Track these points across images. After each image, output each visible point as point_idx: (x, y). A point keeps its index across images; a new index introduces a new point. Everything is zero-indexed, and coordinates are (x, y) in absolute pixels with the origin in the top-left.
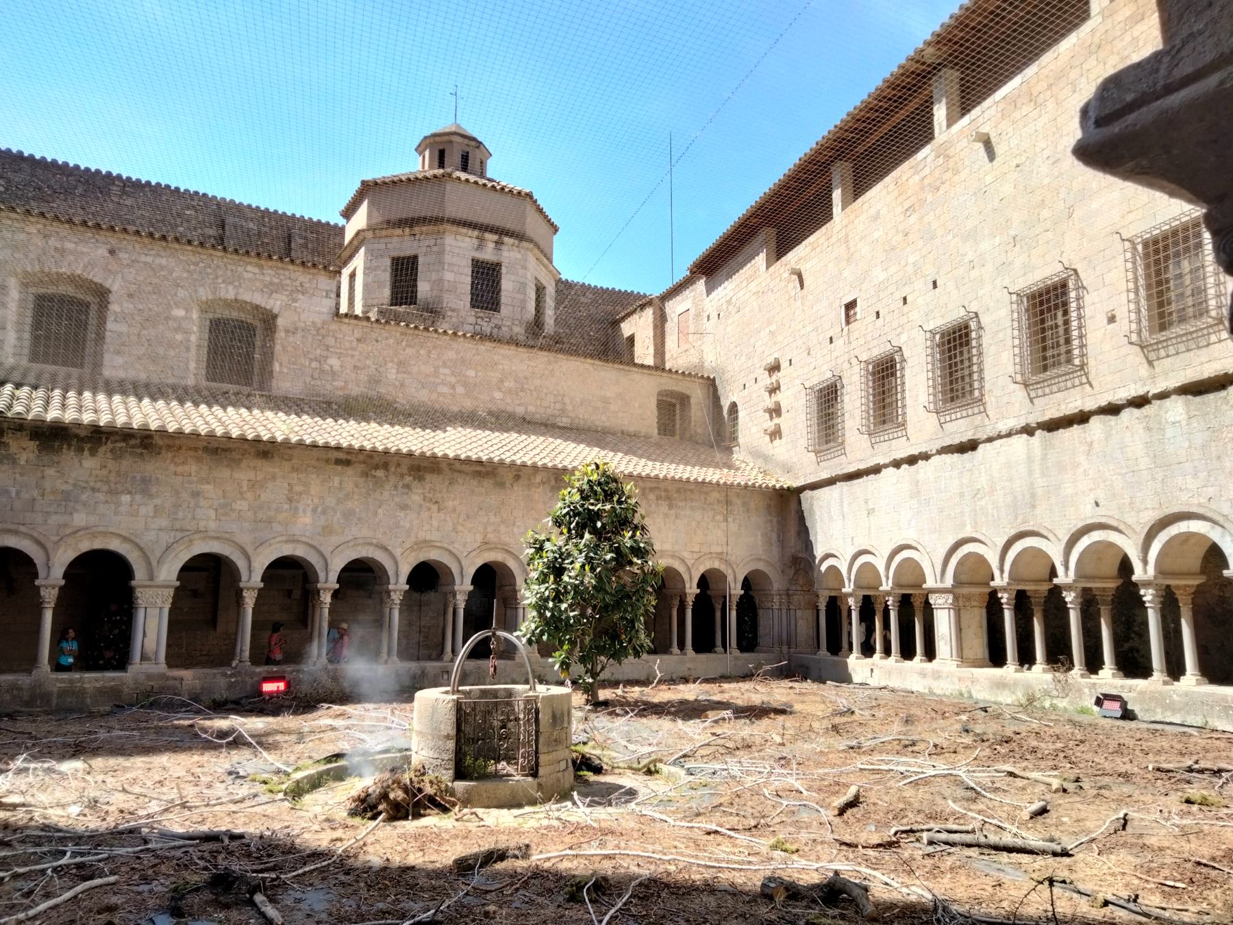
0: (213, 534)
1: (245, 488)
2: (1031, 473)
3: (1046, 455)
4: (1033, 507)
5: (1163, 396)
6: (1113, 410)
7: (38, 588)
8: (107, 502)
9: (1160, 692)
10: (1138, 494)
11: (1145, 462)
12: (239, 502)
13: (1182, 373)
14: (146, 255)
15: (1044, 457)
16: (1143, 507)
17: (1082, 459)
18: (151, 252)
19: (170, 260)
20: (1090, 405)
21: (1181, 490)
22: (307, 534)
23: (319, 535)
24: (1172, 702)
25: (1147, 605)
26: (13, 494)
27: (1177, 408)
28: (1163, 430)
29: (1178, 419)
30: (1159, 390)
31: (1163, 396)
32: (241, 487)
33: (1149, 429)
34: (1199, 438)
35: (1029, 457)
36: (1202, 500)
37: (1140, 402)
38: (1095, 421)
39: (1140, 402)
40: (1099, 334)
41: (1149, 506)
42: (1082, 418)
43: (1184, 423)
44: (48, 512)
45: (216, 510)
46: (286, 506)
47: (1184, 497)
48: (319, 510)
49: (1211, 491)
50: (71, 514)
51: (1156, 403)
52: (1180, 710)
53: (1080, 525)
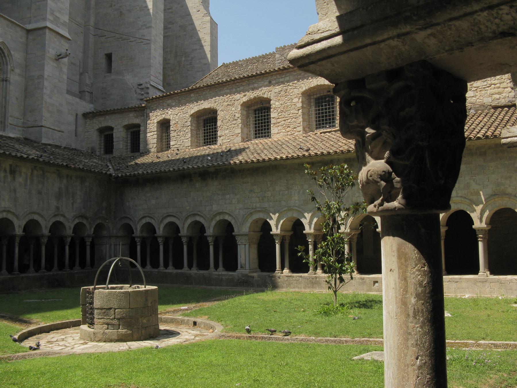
0: (259, 209)
1: (269, 185)
7: (206, 237)
8: (222, 199)
12: (267, 193)
14: (281, 78)
18: (283, 76)
19: (290, 76)
22: (297, 205)
23: (302, 205)
26: (196, 200)
32: (267, 185)
44: (205, 206)
45: (259, 197)
46: (287, 192)
48: (301, 192)
50: (212, 205)
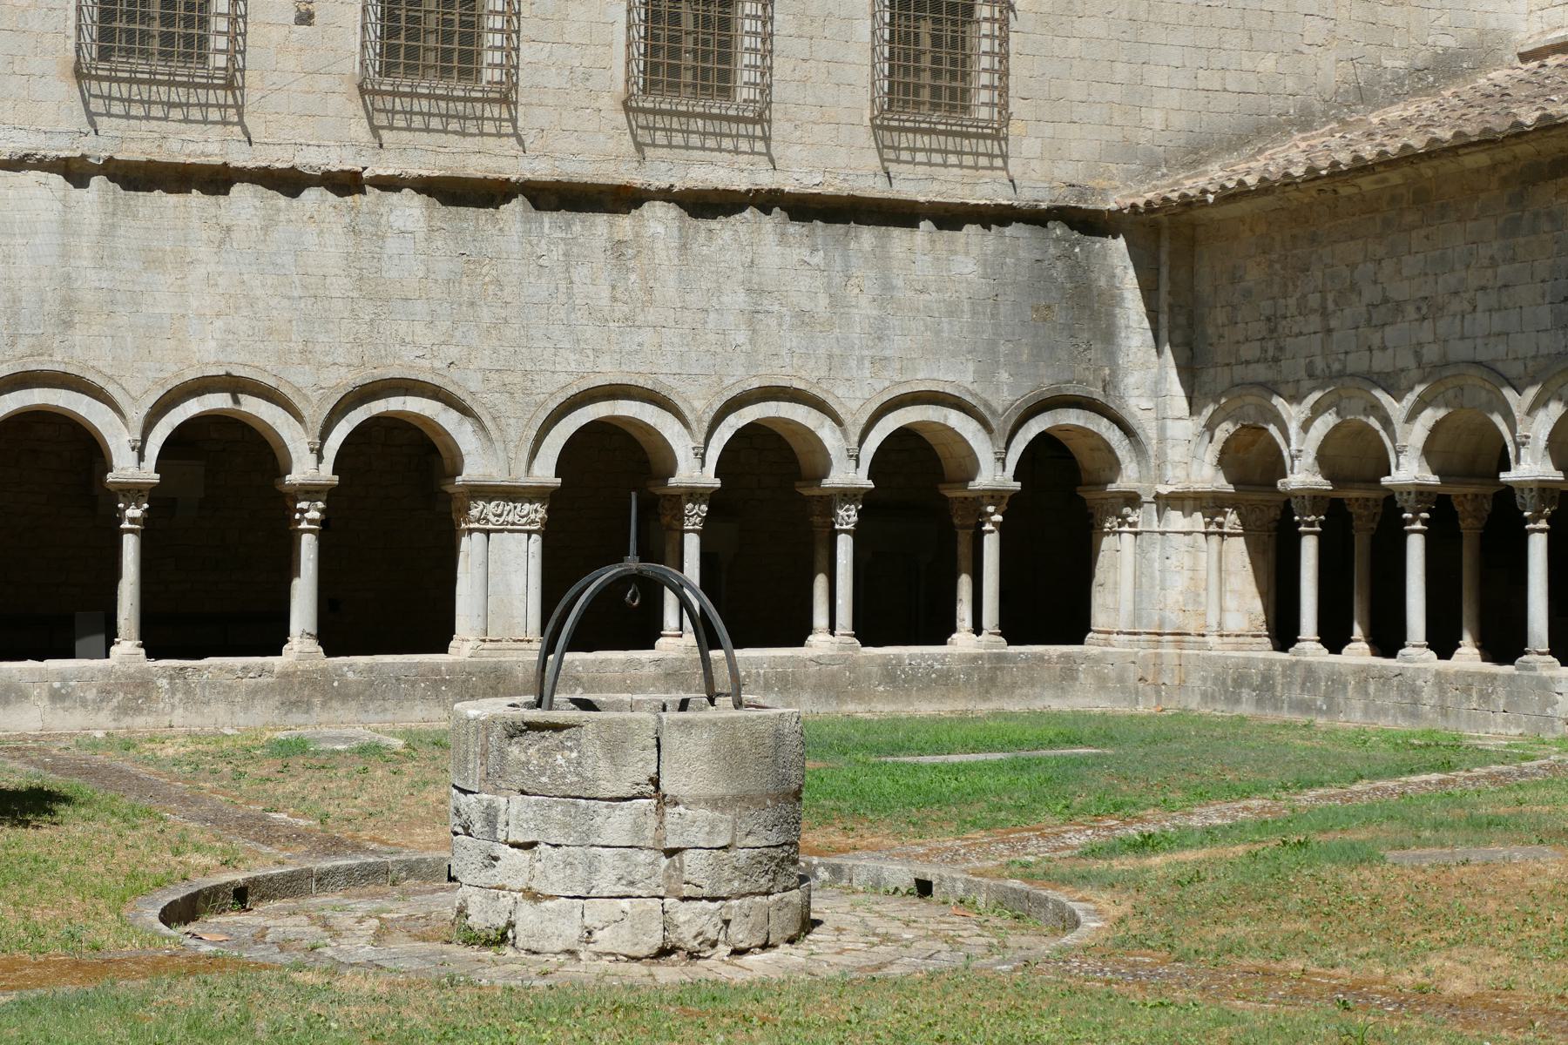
2: (65, 254)
3: (113, 226)
4: (68, 325)
5: (390, 184)
6: (289, 182)
9: (323, 671)
10: (321, 338)
11: (340, 285)
13: (431, 157)
15: (108, 231)
16: (329, 360)
17: (204, 252)
20: (241, 157)
21: (403, 342)
24: (345, 684)
25: (126, 525)
27: (410, 209)
28: (383, 238)
29: (410, 227)
30: (390, 172)
31: (390, 184)
33: (354, 230)
34: (443, 267)
35: (65, 223)
36: (437, 364)
37: (346, 184)
38: (241, 192)
39: (346, 184)
40: (276, 34)
41: (341, 360)
42: (217, 180)
43: (420, 235)
47: (408, 354)
49: (453, 352)
51: (373, 193)
52: (358, 695)
53: (190, 375)
